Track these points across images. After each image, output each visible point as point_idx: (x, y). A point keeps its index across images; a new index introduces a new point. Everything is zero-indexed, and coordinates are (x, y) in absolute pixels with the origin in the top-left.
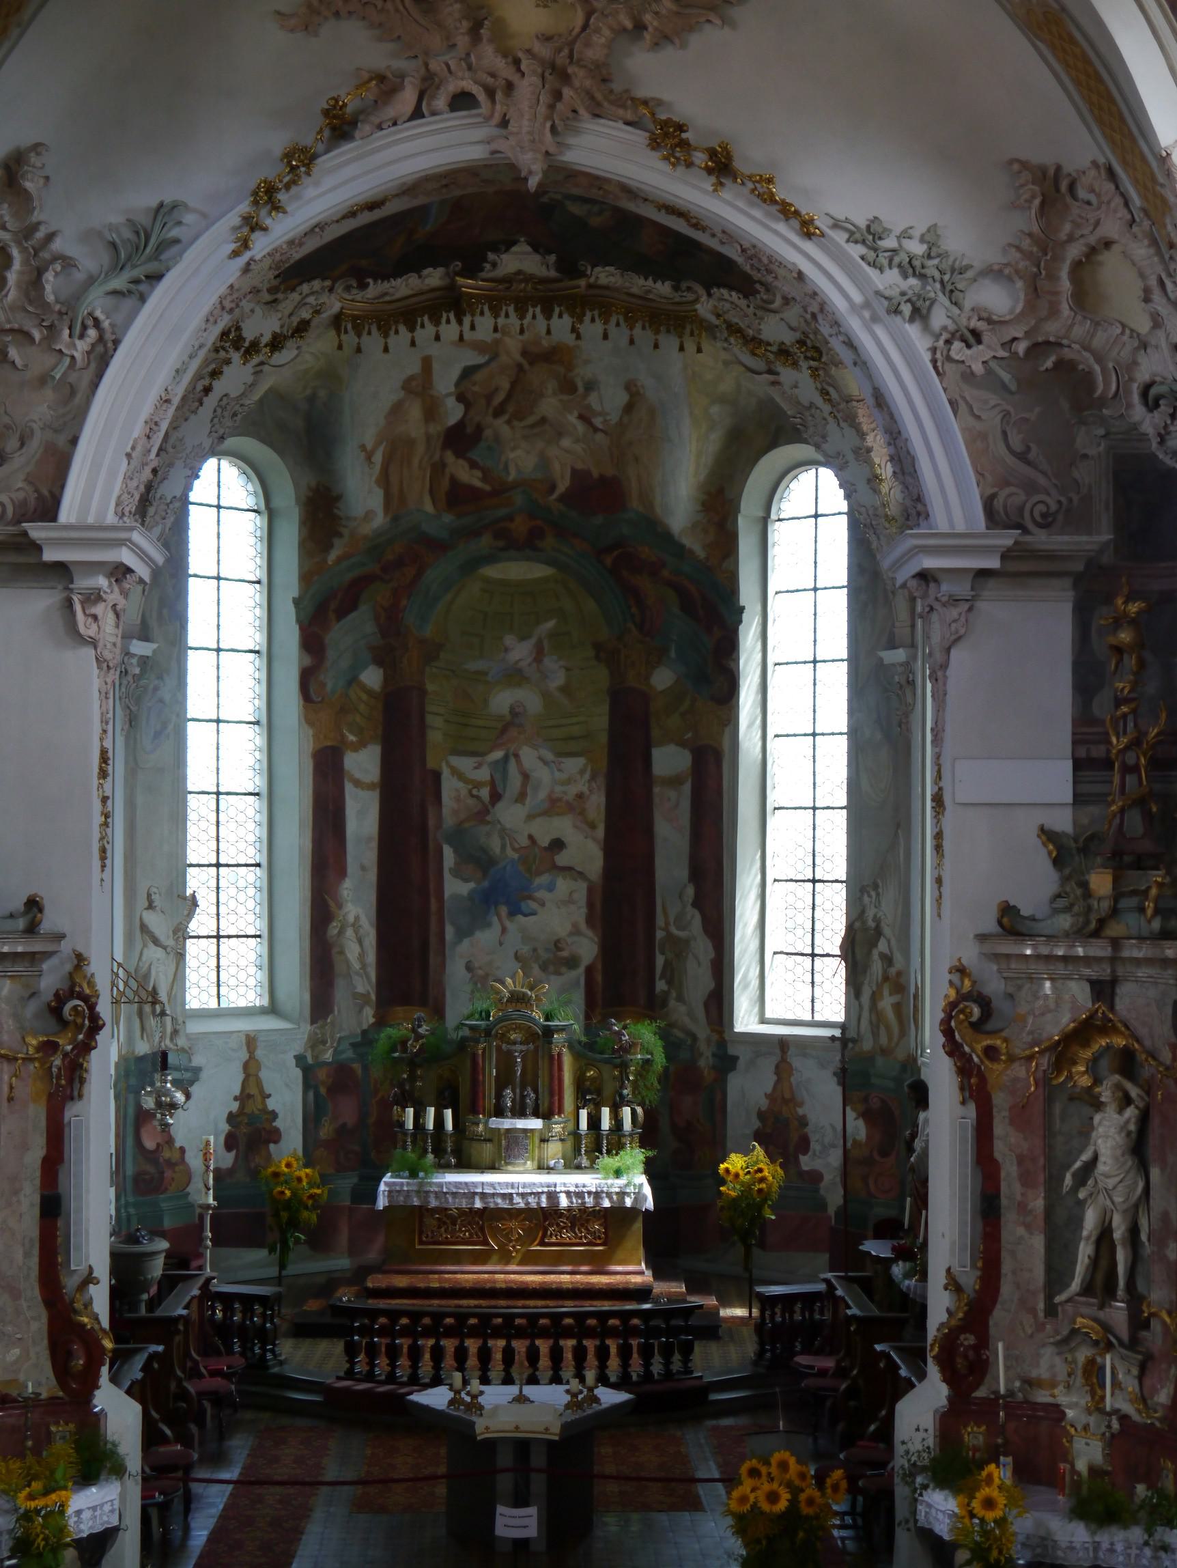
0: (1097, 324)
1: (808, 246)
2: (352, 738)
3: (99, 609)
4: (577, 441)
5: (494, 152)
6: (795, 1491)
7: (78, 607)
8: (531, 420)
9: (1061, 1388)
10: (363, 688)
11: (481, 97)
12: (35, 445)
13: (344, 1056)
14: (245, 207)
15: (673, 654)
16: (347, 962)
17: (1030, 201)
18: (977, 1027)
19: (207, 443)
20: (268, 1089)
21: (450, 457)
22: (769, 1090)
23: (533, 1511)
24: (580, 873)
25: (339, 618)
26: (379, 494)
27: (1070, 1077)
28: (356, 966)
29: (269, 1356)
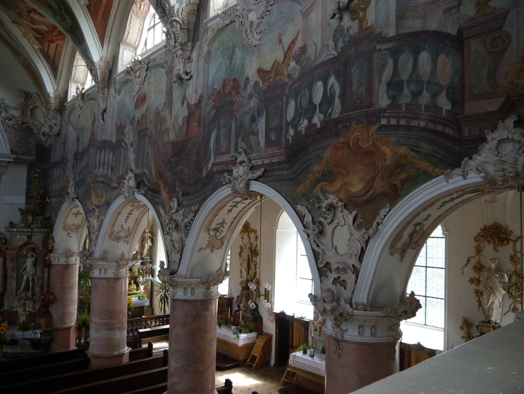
9: (18, 308)
18: (4, 244)
27: (22, 252)
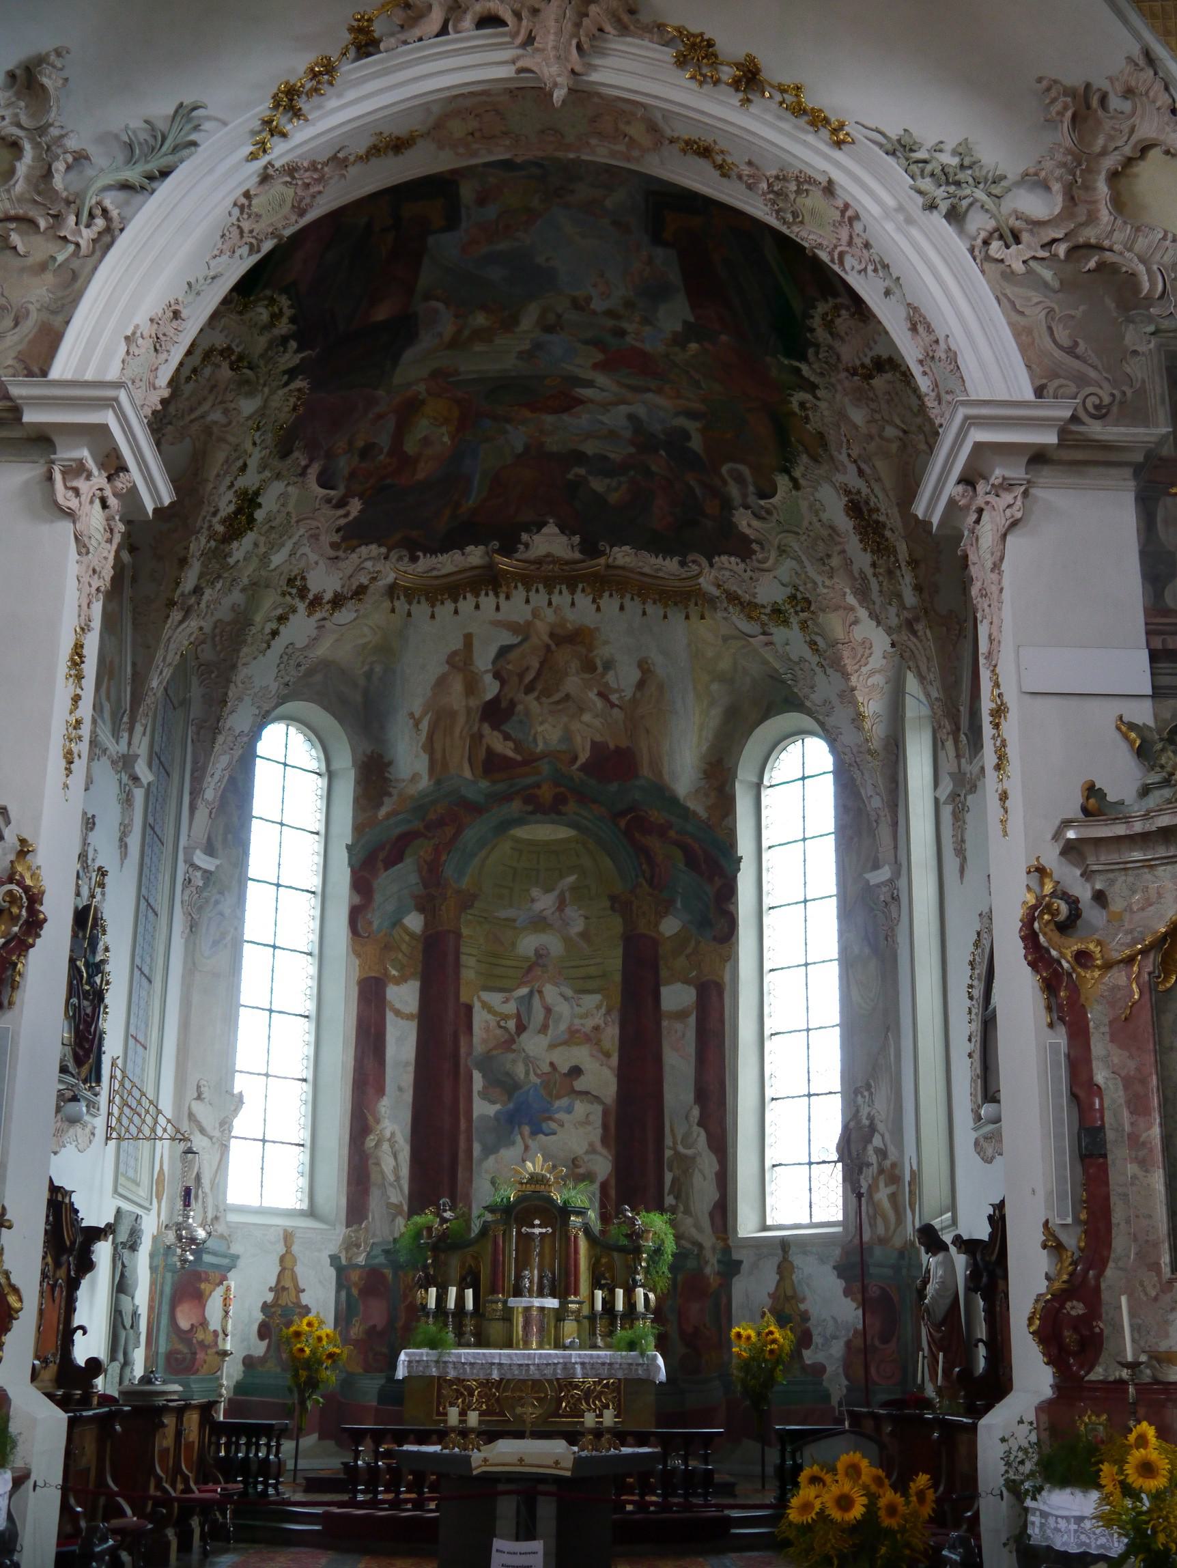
0: (1138, 229)
1: (837, 155)
2: (394, 972)
3: (81, 483)
4: (597, 716)
5: (521, 70)
6: (873, 1498)
7: (58, 476)
8: (556, 697)
10: (406, 930)
11: (508, 17)
12: (29, 326)
13: (377, 1261)
14: (263, 108)
15: (679, 905)
16: (382, 1172)
17: (1061, 114)
19: (274, 687)
20: (302, 1286)
21: (486, 730)
22: (772, 1289)
23: (537, 1545)
24: (596, 1097)
25: (386, 869)
26: (425, 758)
28: (391, 1178)
29: (271, 1491)
